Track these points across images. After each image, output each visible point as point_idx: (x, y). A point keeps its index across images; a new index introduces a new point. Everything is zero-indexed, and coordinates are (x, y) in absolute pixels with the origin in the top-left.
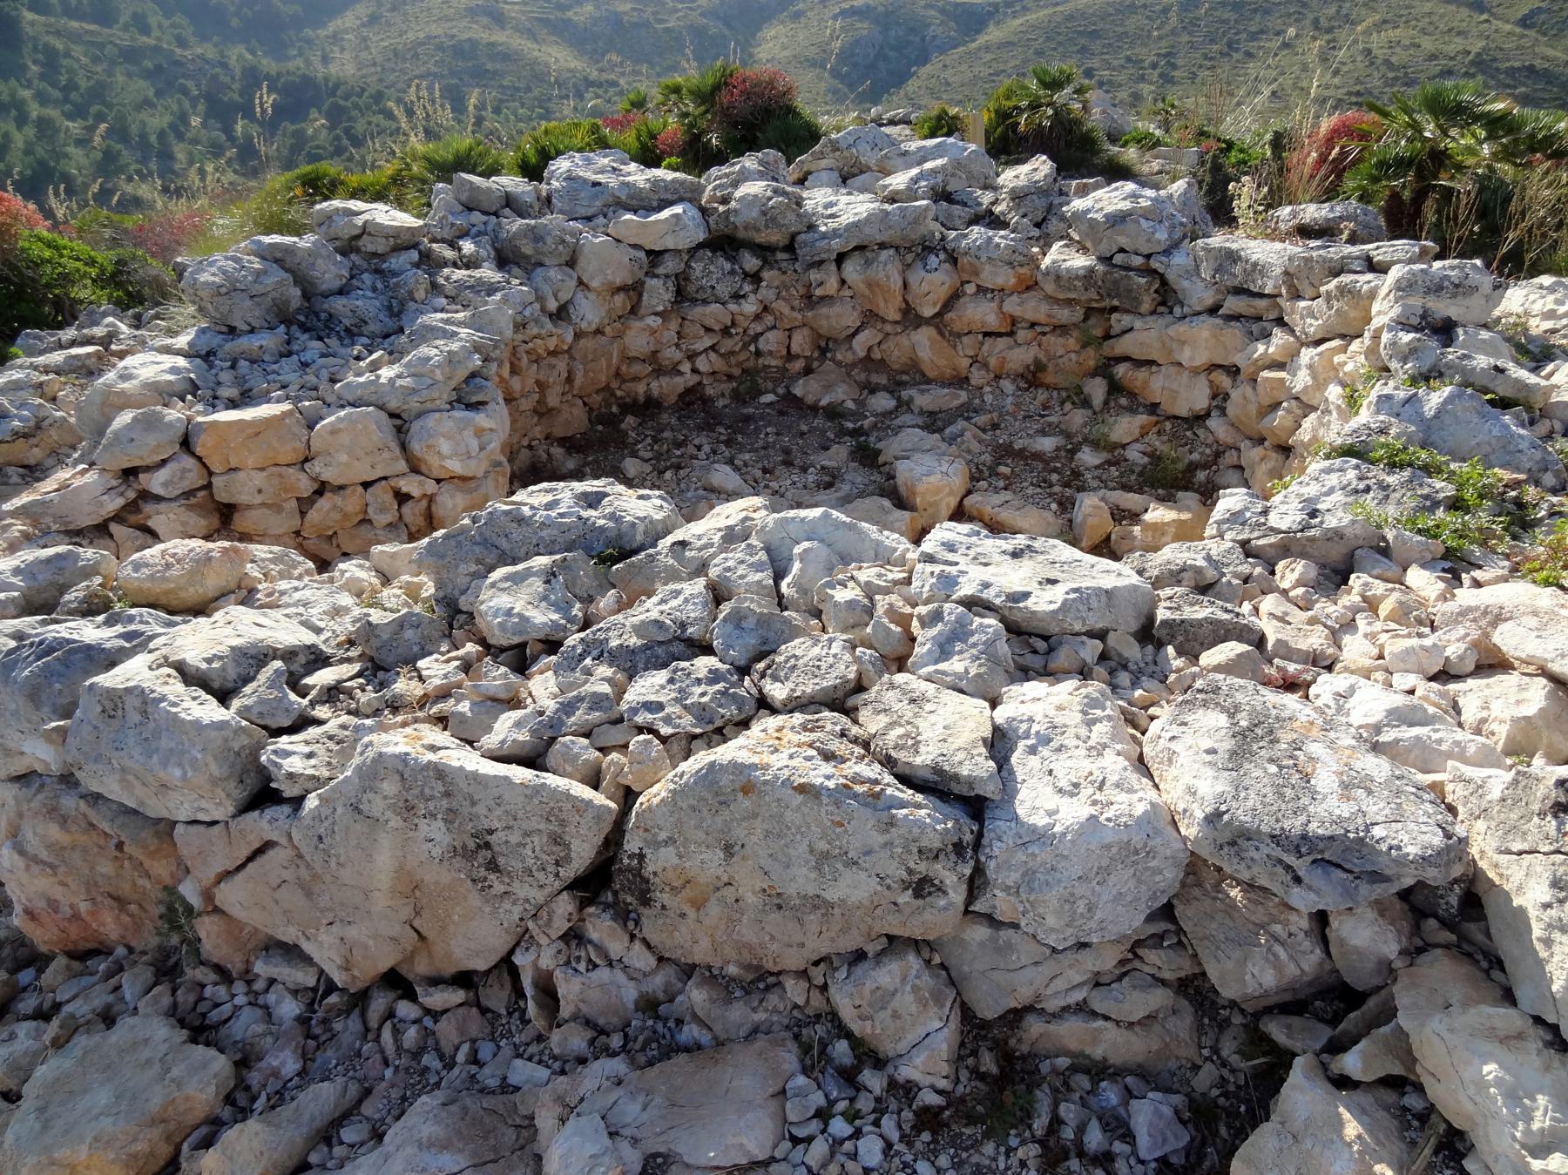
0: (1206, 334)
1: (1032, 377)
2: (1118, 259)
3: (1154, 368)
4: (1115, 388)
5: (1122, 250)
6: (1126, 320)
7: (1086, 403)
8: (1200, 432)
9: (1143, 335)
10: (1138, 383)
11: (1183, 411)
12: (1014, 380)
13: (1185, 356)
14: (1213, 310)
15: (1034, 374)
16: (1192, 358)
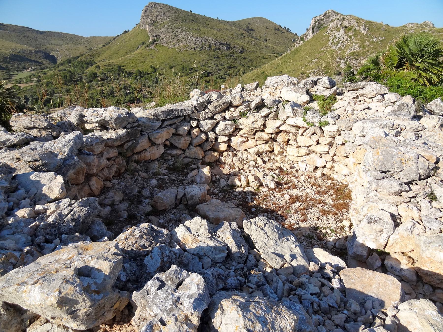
0: (165, 133)
1: (119, 175)
2: (128, 126)
3: (144, 152)
4: (138, 162)
5: (129, 123)
6: (131, 143)
7: (136, 170)
8: (166, 158)
9: (143, 143)
10: (143, 158)
11: (157, 156)
12: (114, 179)
13: (160, 141)
14: (161, 127)
15: (120, 173)
16: (162, 141)
